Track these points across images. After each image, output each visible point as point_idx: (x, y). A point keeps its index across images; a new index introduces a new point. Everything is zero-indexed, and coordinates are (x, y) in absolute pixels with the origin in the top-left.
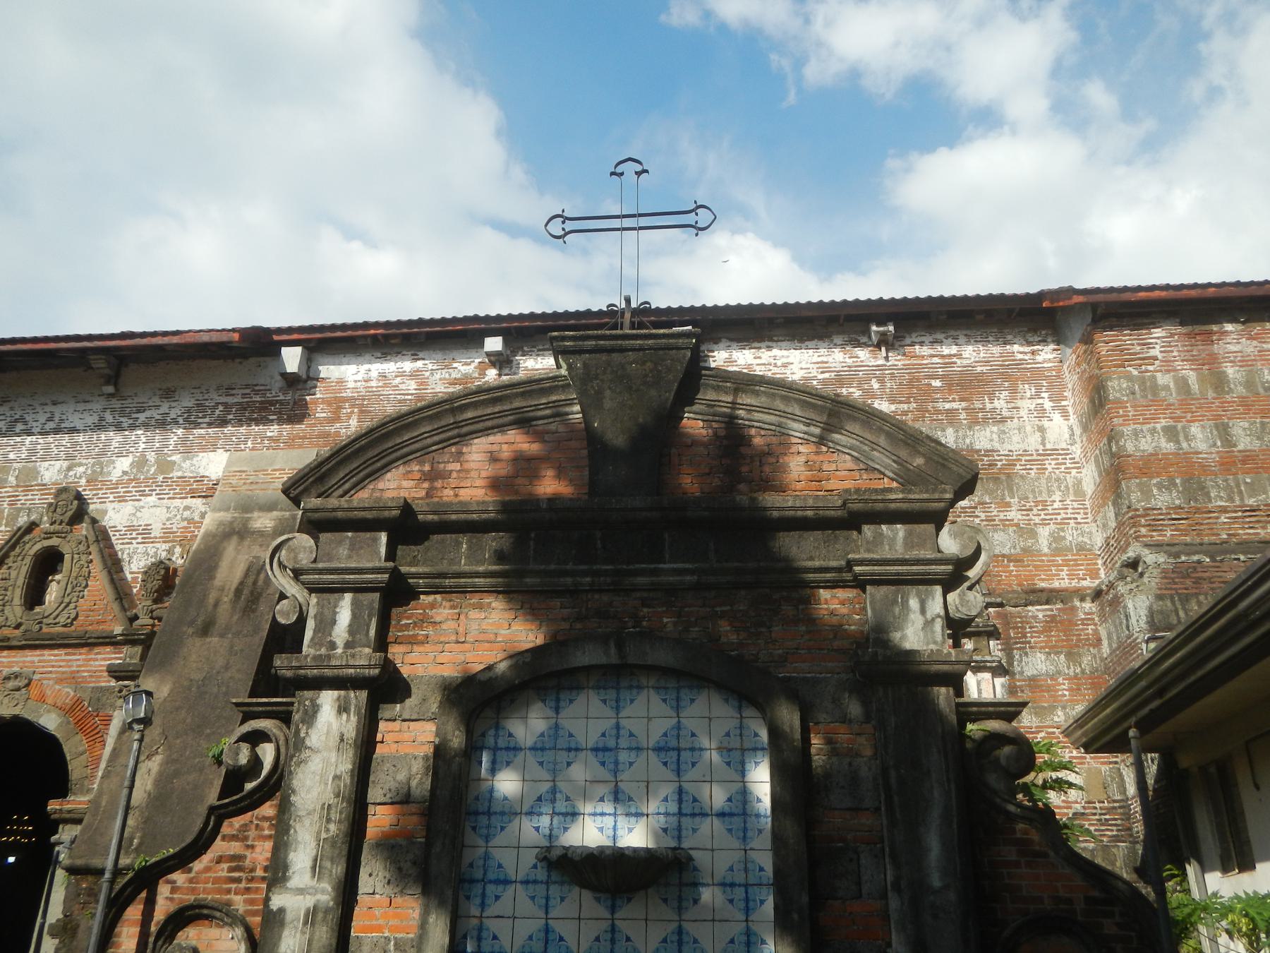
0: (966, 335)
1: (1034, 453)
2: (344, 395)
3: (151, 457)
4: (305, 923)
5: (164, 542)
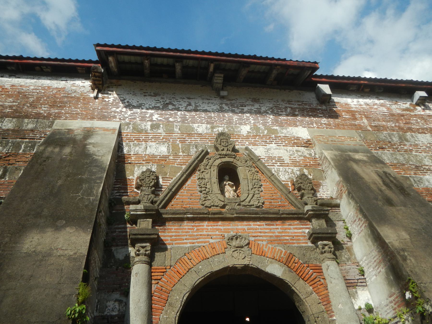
2: (352, 109)
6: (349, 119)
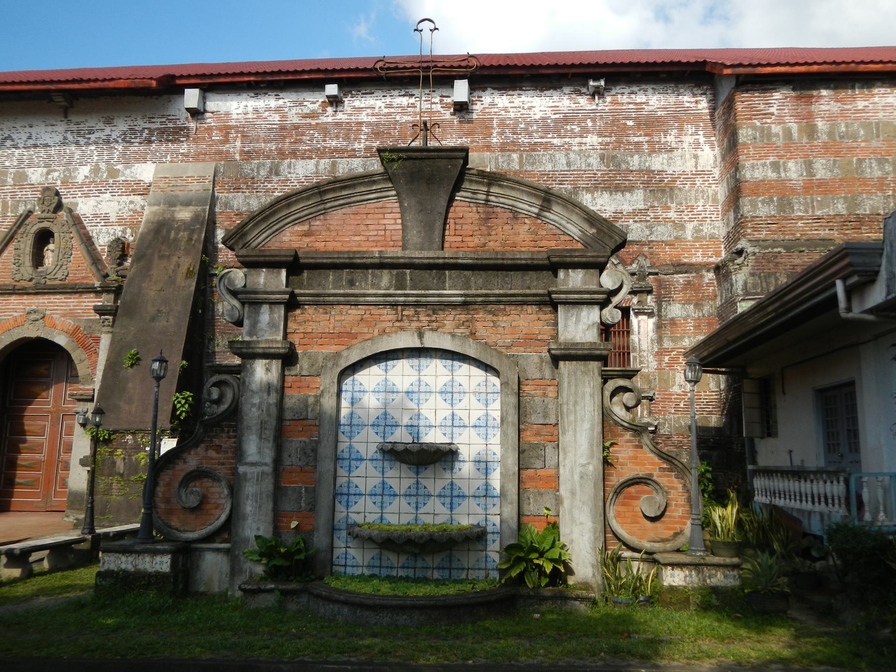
0: (653, 89)
1: (689, 173)
2: (230, 124)
3: (103, 166)
4: (257, 480)
5: (119, 225)
6: (216, 143)
